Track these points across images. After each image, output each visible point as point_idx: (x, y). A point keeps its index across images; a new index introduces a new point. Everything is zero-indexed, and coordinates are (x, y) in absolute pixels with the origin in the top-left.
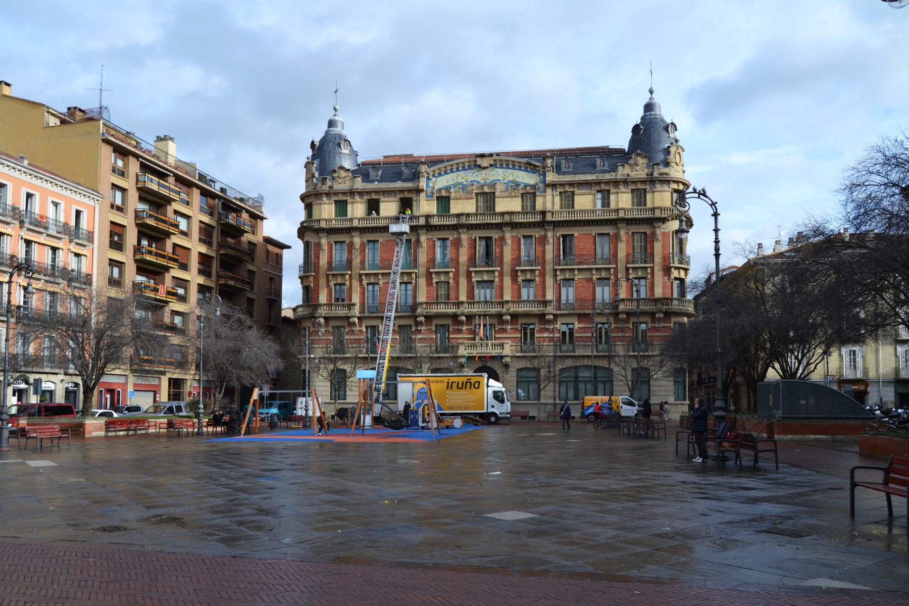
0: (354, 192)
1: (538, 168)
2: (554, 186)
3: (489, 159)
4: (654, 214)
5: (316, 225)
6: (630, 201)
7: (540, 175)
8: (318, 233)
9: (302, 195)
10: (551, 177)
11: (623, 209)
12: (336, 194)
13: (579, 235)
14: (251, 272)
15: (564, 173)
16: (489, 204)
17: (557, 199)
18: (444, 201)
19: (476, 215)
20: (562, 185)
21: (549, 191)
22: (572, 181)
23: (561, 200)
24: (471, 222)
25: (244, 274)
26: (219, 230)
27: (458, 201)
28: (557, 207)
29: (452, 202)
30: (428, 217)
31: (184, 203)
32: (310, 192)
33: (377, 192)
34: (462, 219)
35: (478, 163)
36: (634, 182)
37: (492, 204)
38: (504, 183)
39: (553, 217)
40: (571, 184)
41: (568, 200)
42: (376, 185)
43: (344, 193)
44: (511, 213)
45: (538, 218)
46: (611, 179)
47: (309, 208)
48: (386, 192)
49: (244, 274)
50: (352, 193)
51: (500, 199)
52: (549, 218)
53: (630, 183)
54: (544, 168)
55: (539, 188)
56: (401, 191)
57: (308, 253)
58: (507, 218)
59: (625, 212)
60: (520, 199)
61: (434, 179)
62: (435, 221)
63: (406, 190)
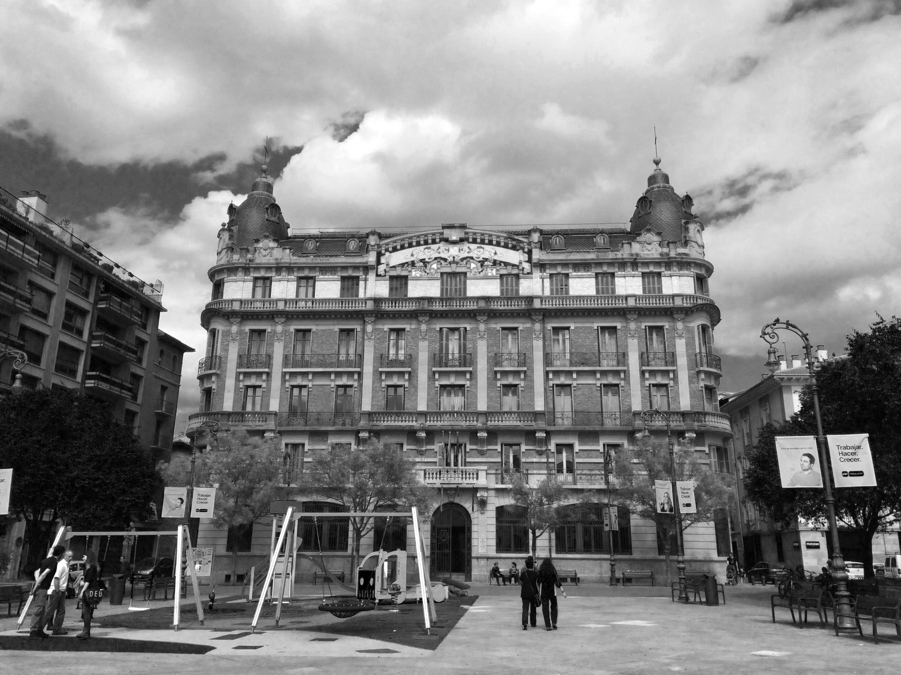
0: (282, 267)
1: (521, 245)
2: (542, 266)
3: (458, 230)
4: (673, 303)
5: (227, 308)
6: (641, 287)
7: (524, 252)
8: (228, 319)
9: (211, 269)
10: (537, 255)
11: (634, 296)
12: (257, 269)
13: (576, 328)
14: (136, 378)
15: (553, 250)
16: (458, 287)
17: (547, 282)
18: (399, 282)
19: (441, 299)
20: (553, 265)
21: (537, 274)
22: (566, 260)
23: (551, 284)
24: (434, 308)
25: (129, 340)
26: (96, 317)
27: (418, 282)
28: (547, 293)
29: (410, 283)
30: (377, 301)
31: (47, 275)
32: (222, 265)
33: (312, 268)
34: (423, 304)
35: (445, 236)
36: (646, 264)
37: (462, 286)
38: (479, 262)
39: (542, 305)
40: (565, 265)
41: (561, 282)
42: (310, 260)
43: (268, 269)
44: (487, 299)
45: (523, 306)
46: (616, 259)
47: (218, 288)
48: (325, 269)
49: (129, 340)
50: (279, 268)
51: (473, 281)
52: (537, 304)
53: (639, 265)
54: (529, 244)
55: (523, 268)
56: (344, 268)
57: (213, 345)
58: (482, 304)
59: (636, 300)
60: (499, 280)
61: (387, 254)
62: (386, 307)
63: (350, 267)
